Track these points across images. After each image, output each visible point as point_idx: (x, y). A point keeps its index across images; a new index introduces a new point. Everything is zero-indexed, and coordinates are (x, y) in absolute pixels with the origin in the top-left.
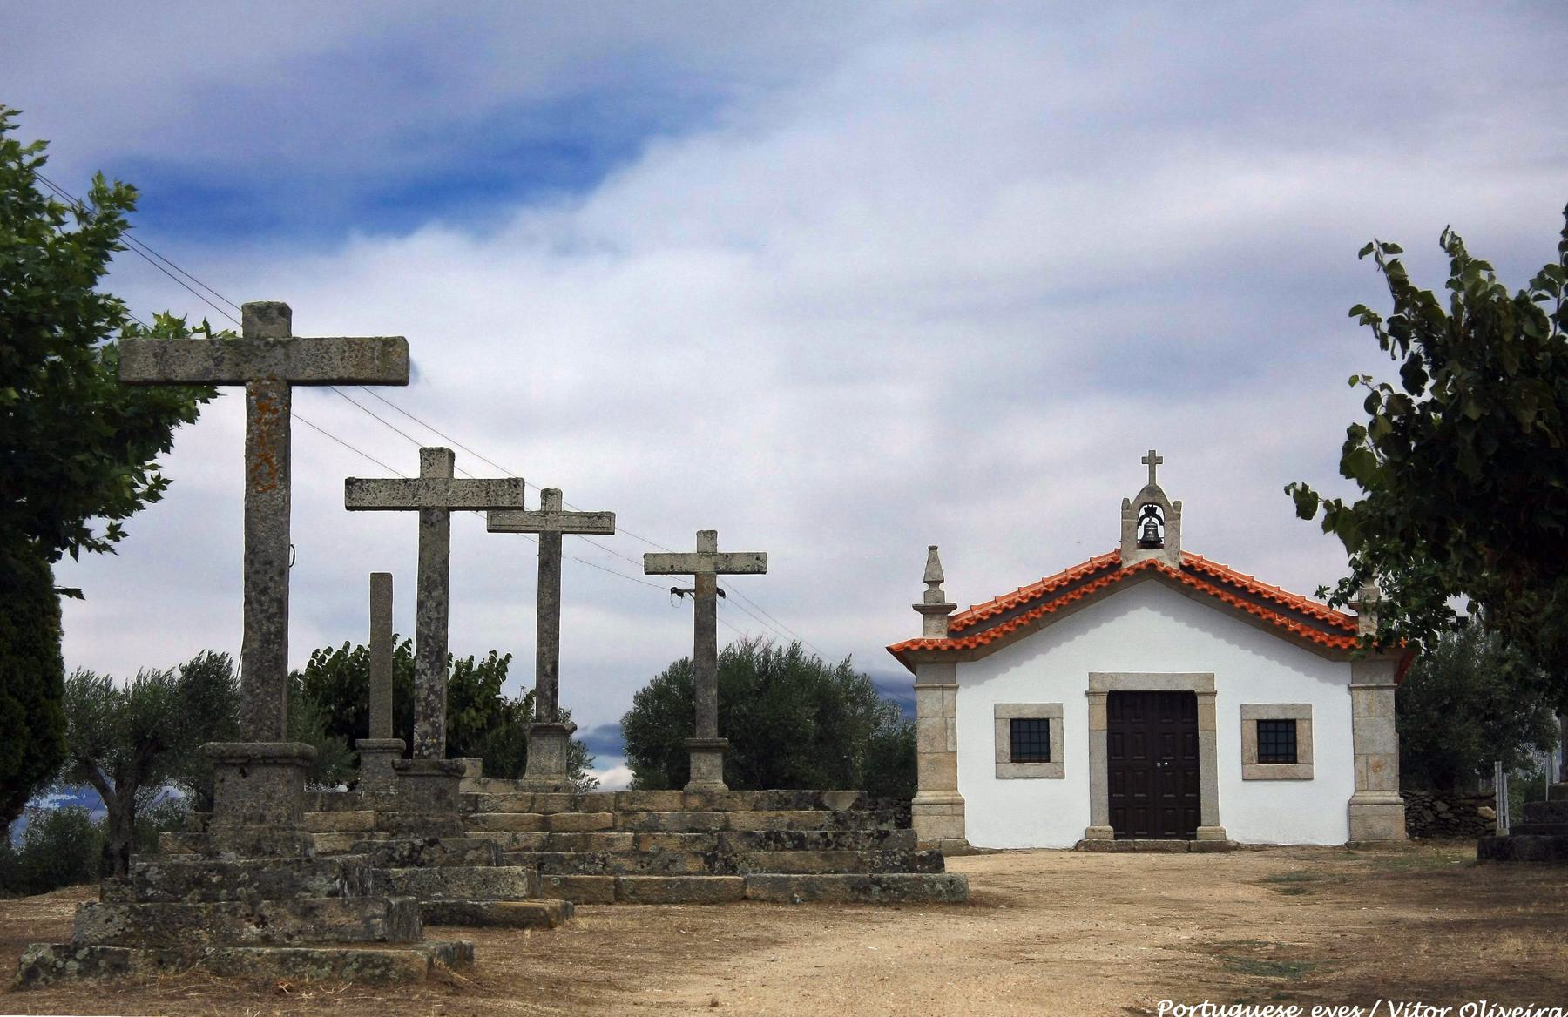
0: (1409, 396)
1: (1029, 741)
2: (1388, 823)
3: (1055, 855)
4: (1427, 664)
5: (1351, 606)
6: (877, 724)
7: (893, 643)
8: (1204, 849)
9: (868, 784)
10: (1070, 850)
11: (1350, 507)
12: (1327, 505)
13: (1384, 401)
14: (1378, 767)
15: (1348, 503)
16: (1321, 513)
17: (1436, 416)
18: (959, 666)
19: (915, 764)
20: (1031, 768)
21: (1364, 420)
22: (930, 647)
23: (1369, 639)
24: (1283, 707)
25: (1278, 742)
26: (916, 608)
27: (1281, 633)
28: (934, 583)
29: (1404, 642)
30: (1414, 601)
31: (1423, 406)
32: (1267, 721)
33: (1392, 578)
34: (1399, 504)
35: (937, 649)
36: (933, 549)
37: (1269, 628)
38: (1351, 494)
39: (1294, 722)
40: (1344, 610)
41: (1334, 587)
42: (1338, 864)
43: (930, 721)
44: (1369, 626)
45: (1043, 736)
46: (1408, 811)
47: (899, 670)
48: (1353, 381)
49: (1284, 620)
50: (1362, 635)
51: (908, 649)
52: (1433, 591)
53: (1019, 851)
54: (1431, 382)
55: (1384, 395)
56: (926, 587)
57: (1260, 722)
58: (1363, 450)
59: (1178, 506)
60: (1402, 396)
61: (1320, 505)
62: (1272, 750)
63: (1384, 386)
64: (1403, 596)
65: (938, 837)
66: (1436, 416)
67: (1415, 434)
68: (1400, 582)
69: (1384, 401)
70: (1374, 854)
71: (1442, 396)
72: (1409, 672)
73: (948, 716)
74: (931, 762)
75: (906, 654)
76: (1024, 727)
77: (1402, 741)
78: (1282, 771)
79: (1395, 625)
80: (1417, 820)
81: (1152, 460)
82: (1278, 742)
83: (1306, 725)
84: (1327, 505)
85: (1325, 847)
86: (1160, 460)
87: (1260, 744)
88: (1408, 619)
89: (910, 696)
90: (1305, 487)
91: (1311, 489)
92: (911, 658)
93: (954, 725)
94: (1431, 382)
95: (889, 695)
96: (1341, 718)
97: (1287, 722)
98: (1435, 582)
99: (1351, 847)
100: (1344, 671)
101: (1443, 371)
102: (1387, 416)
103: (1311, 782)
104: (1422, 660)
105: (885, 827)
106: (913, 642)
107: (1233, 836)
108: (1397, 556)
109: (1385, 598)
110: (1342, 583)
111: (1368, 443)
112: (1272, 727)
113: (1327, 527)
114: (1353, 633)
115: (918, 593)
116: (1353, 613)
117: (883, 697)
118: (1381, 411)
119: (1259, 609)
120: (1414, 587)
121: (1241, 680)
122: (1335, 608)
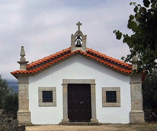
0: (145, 8)
1: (47, 97)
2: (140, 118)
3: (54, 126)
4: (150, 77)
5: (130, 62)
6: (8, 92)
7: (12, 72)
8: (92, 125)
9: (6, 108)
10: (58, 125)
11: (130, 36)
12: (124, 36)
13: (139, 9)
14: (137, 103)
15: (130, 35)
16: (123, 38)
17: (152, 13)
18: (29, 77)
19: (18, 103)
20: (48, 104)
21: (134, 14)
22: (22, 72)
23: (135, 70)
24: (113, 88)
25: (111, 97)
26: (18, 62)
27: (112, 69)
28: (23, 56)
29: (144, 71)
30: (147, 61)
31: (149, 10)
32: (109, 92)
33: (141, 55)
34: (143, 35)
35: (23, 73)
36: (22, 47)
37: (109, 67)
38: (130, 33)
39: (116, 92)
40: (129, 63)
41: (126, 57)
42: (127, 128)
43: (22, 92)
44: (135, 67)
45: (51, 95)
46: (145, 115)
47: (14, 78)
48: (131, 4)
49: (113, 65)
50: (133, 69)
51: (16, 73)
52: (151, 58)
53: (45, 125)
54: (151, 4)
55: (139, 7)
56: (21, 57)
57: (107, 92)
58: (134, 21)
59: (86, 36)
60: (143, 8)
61: (122, 36)
62: (110, 99)
63: (139, 5)
64: (144, 59)
65: (24, 122)
66: (152, 13)
67: (147, 17)
68: (143, 56)
69: (139, 9)
70: (136, 126)
71: (154, 8)
72: (145, 79)
73: (26, 90)
74: (22, 102)
75: (15, 74)
76: (46, 93)
77: (144, 97)
78: (113, 104)
79: (142, 67)
80: (147, 117)
81: (79, 24)
82: (111, 97)
83: (119, 92)
84: (124, 36)
85: (124, 124)
86: (81, 24)
87: (107, 97)
88: (145, 65)
89: (17, 85)
90: (118, 31)
91: (120, 32)
92: (17, 75)
93: (28, 92)
94: (151, 4)
95: (11, 85)
96: (127, 90)
97: (114, 92)
98: (152, 56)
99: (130, 124)
100: (129, 79)
101: (154, 1)
102: (140, 13)
103: (120, 109)
104: (149, 76)
105: (10, 119)
106: (17, 71)
107: (100, 121)
108: (142, 49)
109: (139, 60)
110: (128, 56)
111: (135, 20)
112: (110, 93)
113: (124, 42)
114: (131, 69)
115: (19, 59)
116: (131, 64)
117: (10, 85)
118: (138, 11)
119: (107, 63)
120: (146, 57)
121: (102, 81)
122: (126, 62)
